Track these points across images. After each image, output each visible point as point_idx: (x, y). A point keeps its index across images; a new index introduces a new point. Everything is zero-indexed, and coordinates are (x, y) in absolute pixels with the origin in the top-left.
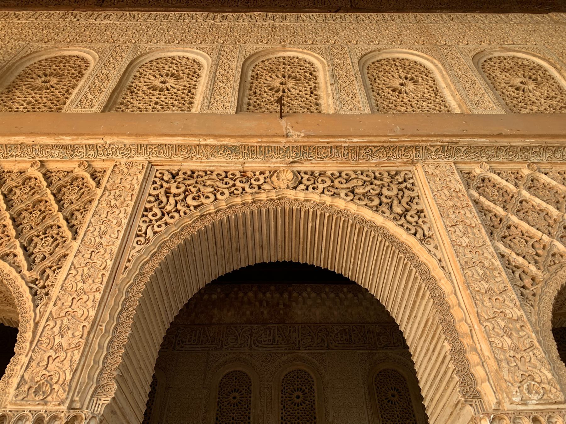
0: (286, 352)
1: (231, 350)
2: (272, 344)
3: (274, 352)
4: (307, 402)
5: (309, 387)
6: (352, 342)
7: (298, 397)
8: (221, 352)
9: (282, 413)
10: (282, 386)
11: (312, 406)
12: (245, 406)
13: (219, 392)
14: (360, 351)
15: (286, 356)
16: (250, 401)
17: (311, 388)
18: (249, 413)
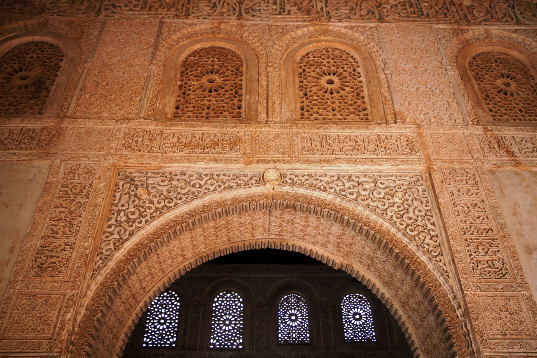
0: (305, 24)
1: (204, 18)
2: (280, 14)
3: (285, 23)
4: (347, 89)
5: (351, 70)
6: (423, 14)
7: (331, 82)
8: (186, 21)
9: (303, 102)
10: (301, 67)
11: (358, 95)
12: (230, 92)
13: (182, 72)
14: (440, 26)
15: (305, 30)
16: (241, 85)
17: (354, 71)
18: (240, 101)
